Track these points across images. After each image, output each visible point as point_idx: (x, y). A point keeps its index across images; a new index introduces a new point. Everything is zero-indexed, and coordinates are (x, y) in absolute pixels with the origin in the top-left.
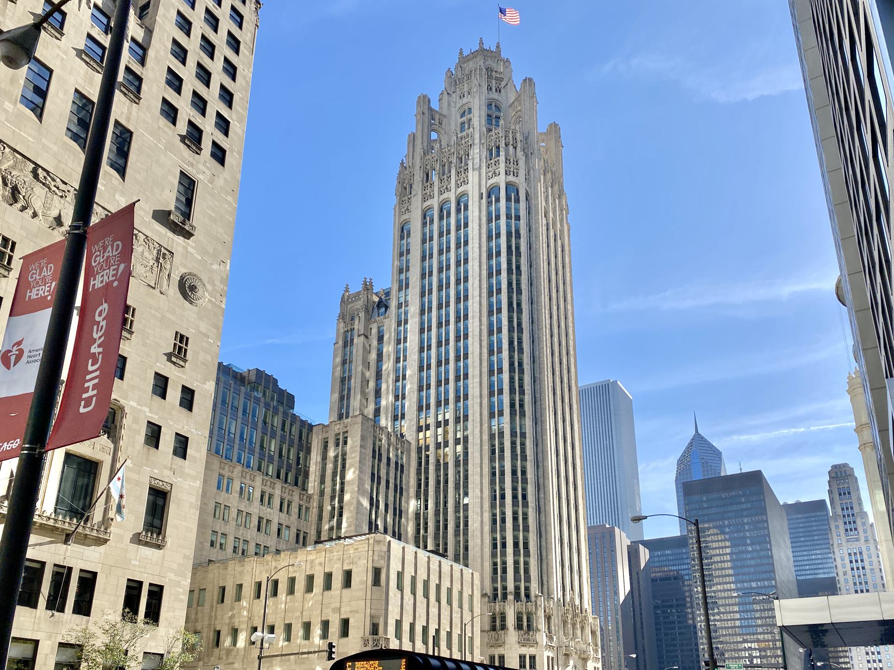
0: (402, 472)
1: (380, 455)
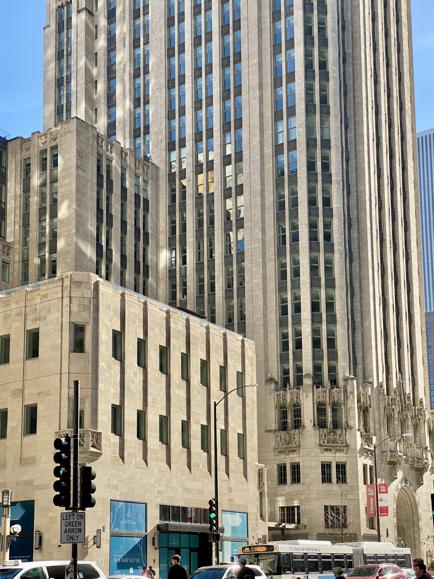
0: (146, 209)
1: (110, 182)
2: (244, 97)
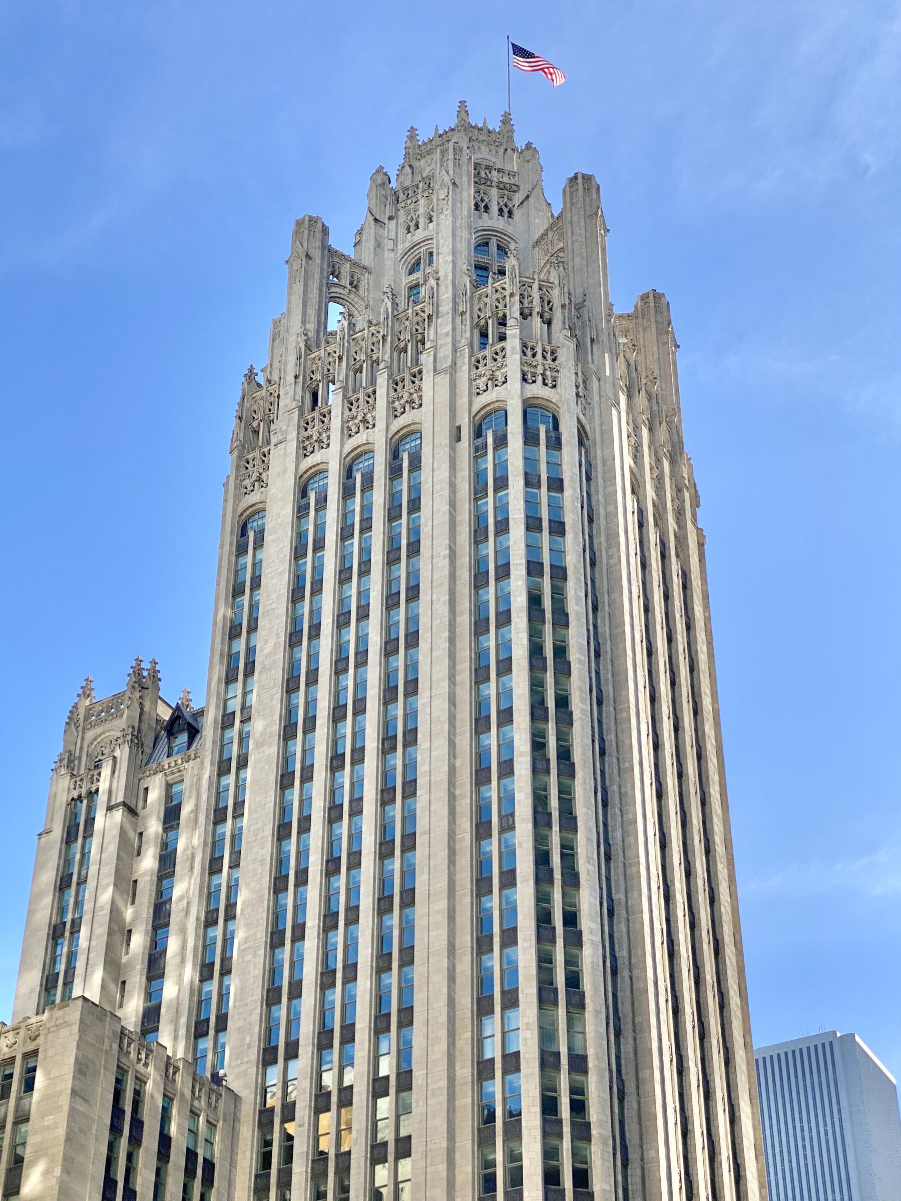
0: (208, 1181)
1: (137, 1124)
2: (419, 970)
